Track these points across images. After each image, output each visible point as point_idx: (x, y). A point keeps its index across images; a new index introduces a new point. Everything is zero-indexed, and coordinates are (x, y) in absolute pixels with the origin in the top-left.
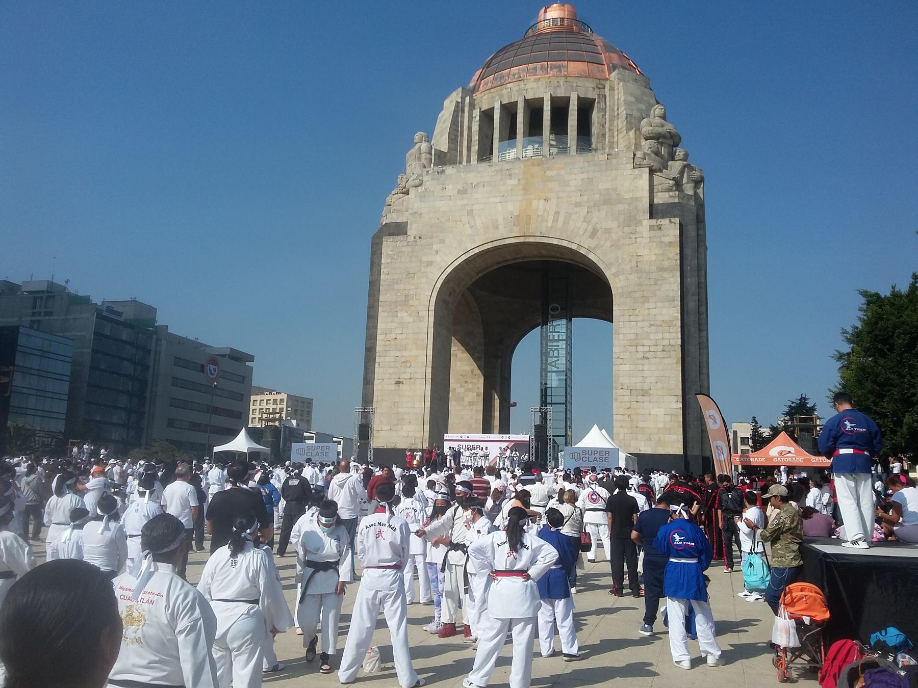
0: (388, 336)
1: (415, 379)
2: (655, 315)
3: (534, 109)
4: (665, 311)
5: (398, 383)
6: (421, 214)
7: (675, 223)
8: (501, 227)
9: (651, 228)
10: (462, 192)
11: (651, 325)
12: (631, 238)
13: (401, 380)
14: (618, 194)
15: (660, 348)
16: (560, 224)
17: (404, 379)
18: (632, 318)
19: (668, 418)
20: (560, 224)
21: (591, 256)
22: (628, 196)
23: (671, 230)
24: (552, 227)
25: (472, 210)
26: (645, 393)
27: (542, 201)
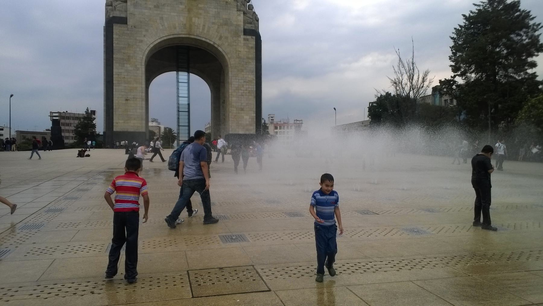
0: (120, 76)
1: (137, 98)
2: (246, 78)
4: (250, 76)
5: (127, 100)
6: (134, 15)
7: (253, 39)
9: (245, 39)
11: (244, 82)
12: (236, 43)
13: (128, 99)
14: (231, 21)
15: (248, 92)
16: (205, 31)
17: (130, 98)
19: (250, 120)
20: (205, 31)
21: (220, 49)
22: (235, 23)
24: (202, 32)
26: (242, 109)
27: (197, 19)
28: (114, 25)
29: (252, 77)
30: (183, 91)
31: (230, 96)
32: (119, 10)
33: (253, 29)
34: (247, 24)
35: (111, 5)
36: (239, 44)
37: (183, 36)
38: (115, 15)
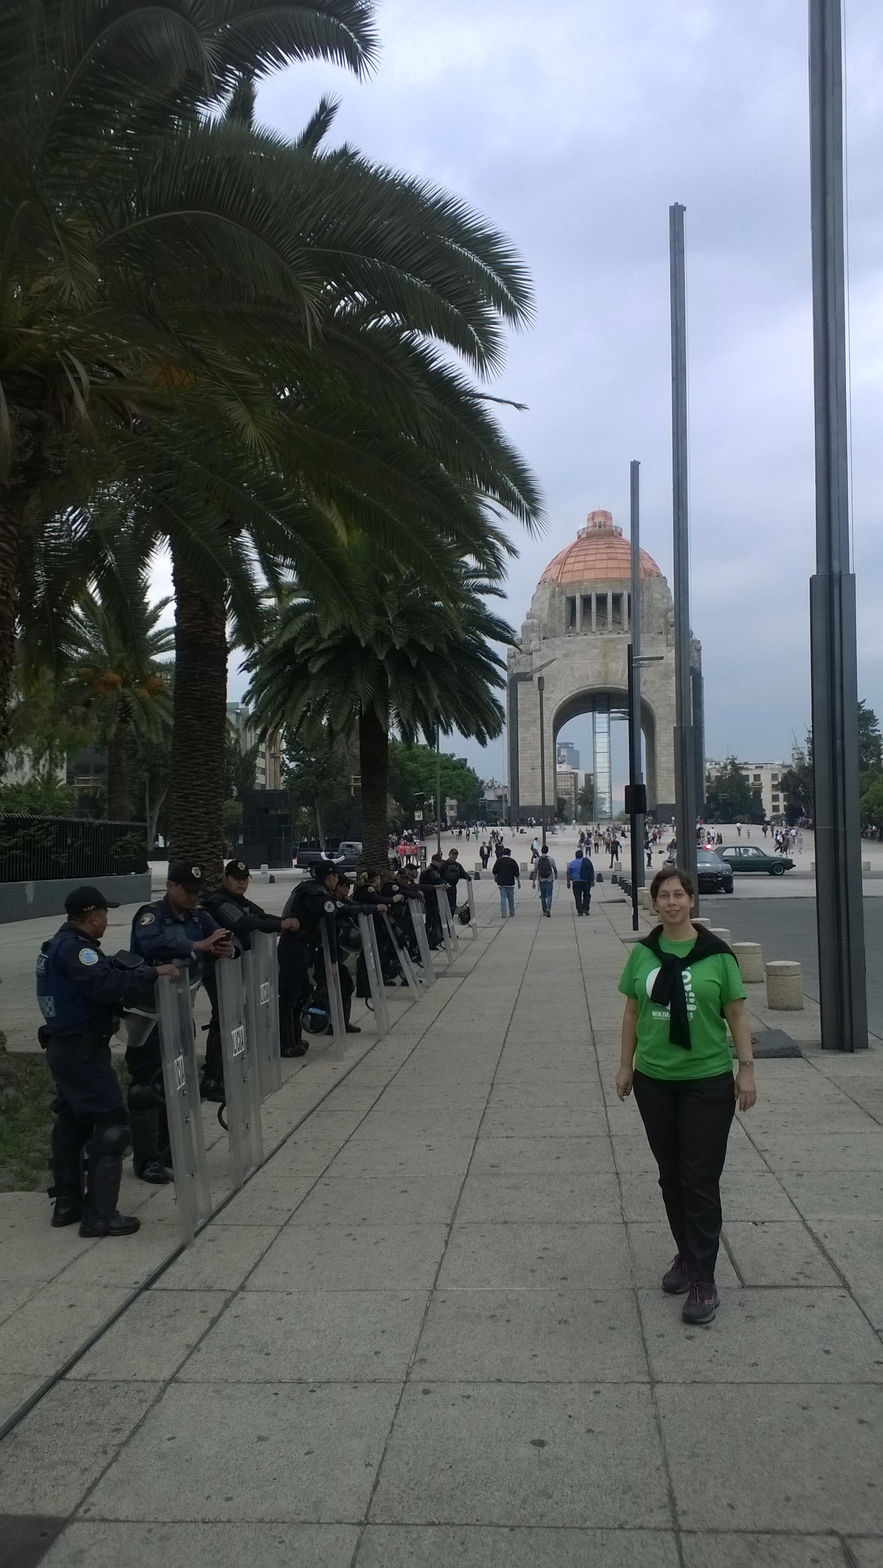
5: (533, 769)
8: (590, 677)
10: (566, 656)
18: (668, 731)
31: (659, 755)
32: (524, 665)
35: (514, 657)
37: (598, 686)
38: (519, 671)
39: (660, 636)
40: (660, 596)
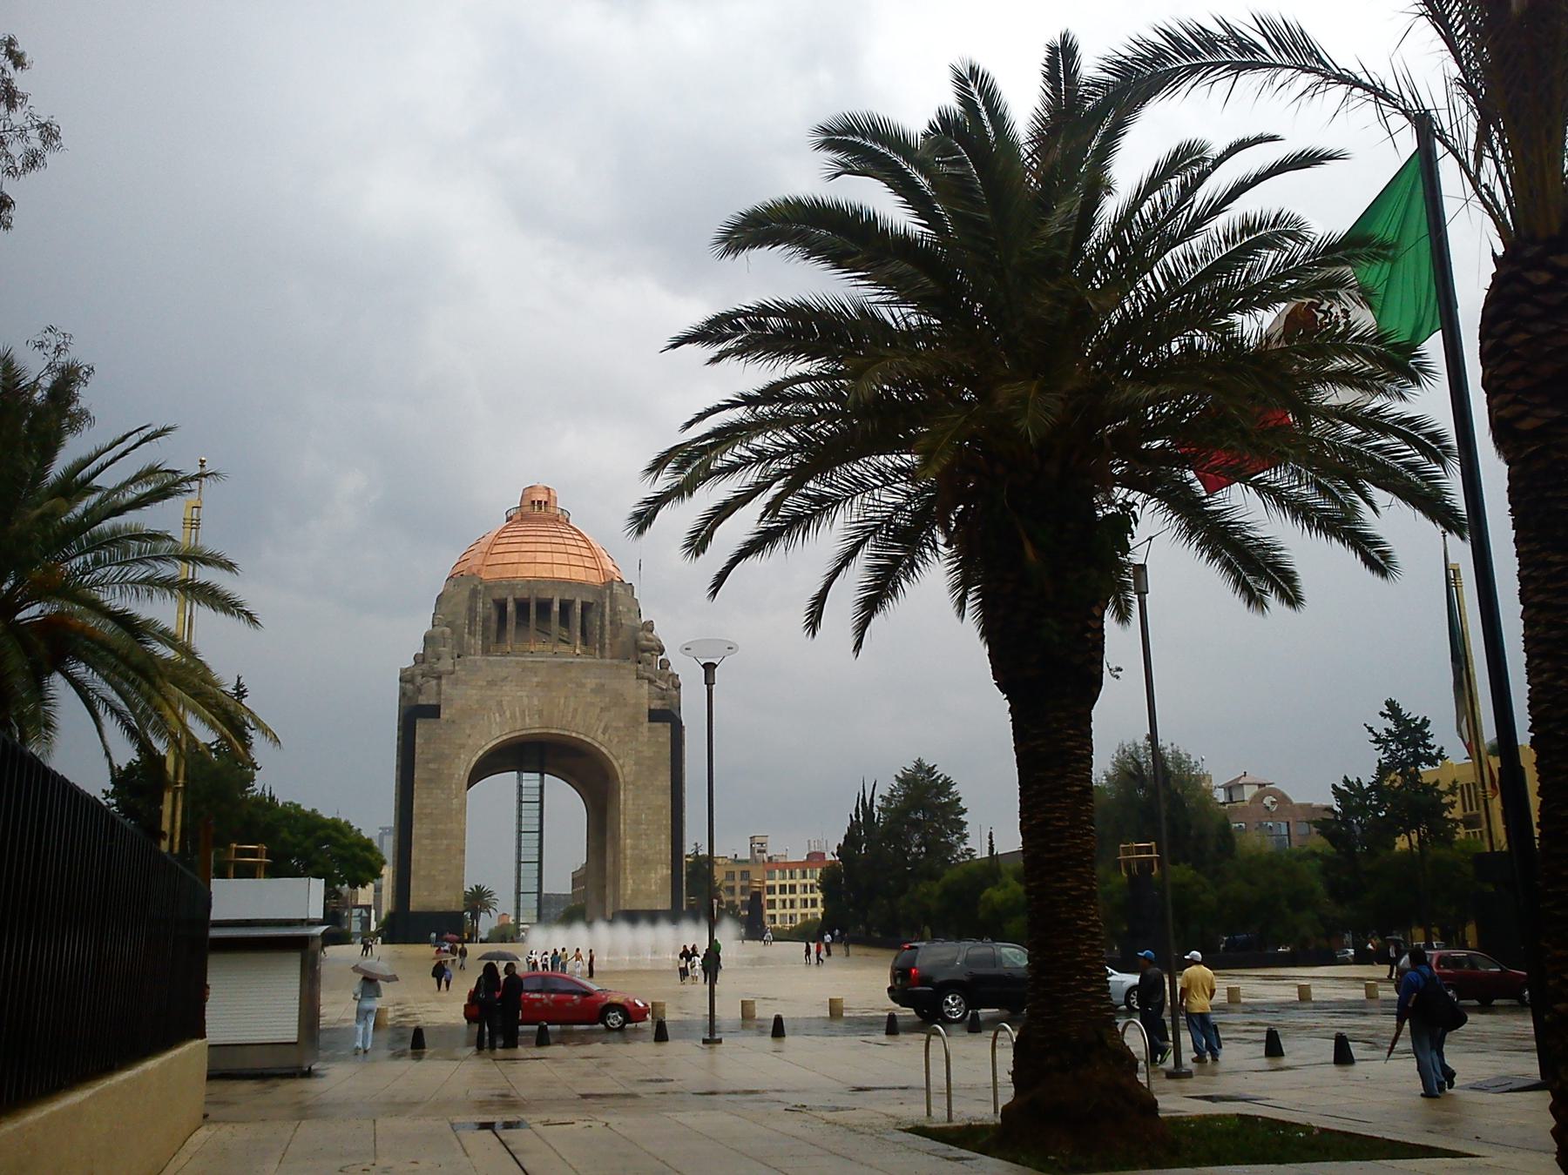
3: (544, 607)
21: (603, 749)
22: (633, 701)
23: (664, 731)
25: (501, 701)
28: (417, 721)
29: (666, 800)
30: (531, 823)
33: (668, 708)
34: (655, 701)
36: (640, 739)
37: (537, 731)
39: (630, 666)
40: (625, 610)
